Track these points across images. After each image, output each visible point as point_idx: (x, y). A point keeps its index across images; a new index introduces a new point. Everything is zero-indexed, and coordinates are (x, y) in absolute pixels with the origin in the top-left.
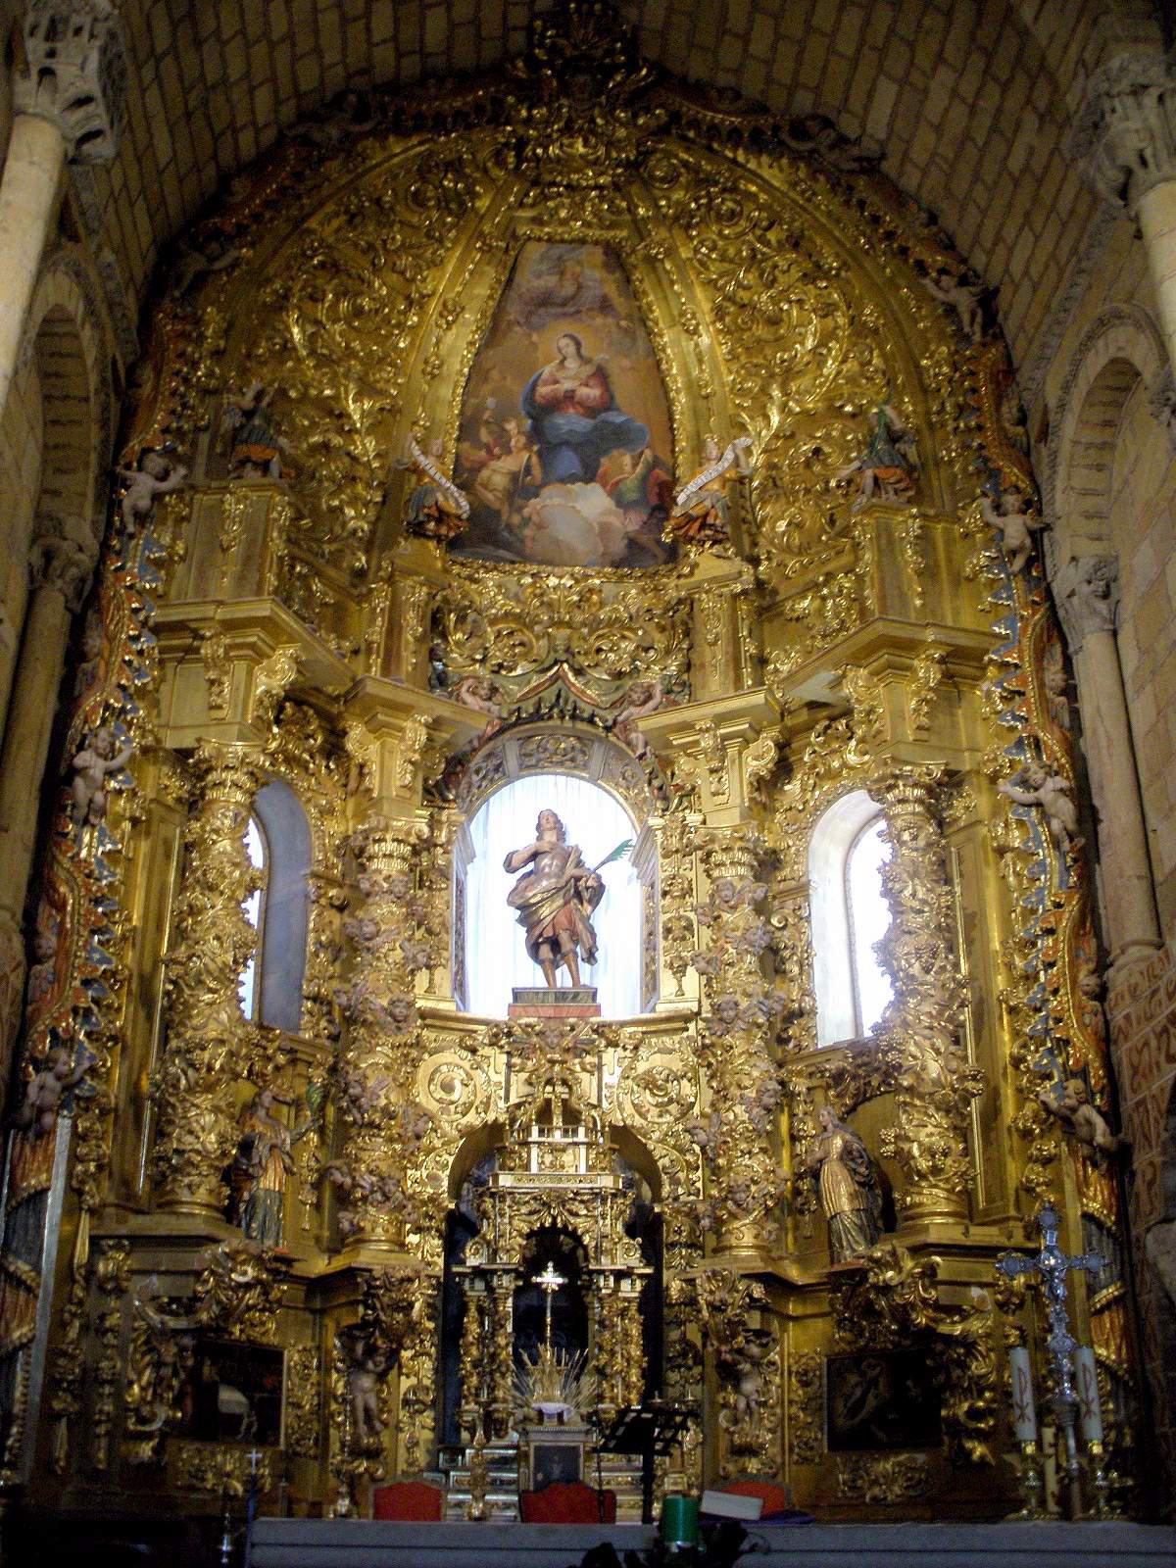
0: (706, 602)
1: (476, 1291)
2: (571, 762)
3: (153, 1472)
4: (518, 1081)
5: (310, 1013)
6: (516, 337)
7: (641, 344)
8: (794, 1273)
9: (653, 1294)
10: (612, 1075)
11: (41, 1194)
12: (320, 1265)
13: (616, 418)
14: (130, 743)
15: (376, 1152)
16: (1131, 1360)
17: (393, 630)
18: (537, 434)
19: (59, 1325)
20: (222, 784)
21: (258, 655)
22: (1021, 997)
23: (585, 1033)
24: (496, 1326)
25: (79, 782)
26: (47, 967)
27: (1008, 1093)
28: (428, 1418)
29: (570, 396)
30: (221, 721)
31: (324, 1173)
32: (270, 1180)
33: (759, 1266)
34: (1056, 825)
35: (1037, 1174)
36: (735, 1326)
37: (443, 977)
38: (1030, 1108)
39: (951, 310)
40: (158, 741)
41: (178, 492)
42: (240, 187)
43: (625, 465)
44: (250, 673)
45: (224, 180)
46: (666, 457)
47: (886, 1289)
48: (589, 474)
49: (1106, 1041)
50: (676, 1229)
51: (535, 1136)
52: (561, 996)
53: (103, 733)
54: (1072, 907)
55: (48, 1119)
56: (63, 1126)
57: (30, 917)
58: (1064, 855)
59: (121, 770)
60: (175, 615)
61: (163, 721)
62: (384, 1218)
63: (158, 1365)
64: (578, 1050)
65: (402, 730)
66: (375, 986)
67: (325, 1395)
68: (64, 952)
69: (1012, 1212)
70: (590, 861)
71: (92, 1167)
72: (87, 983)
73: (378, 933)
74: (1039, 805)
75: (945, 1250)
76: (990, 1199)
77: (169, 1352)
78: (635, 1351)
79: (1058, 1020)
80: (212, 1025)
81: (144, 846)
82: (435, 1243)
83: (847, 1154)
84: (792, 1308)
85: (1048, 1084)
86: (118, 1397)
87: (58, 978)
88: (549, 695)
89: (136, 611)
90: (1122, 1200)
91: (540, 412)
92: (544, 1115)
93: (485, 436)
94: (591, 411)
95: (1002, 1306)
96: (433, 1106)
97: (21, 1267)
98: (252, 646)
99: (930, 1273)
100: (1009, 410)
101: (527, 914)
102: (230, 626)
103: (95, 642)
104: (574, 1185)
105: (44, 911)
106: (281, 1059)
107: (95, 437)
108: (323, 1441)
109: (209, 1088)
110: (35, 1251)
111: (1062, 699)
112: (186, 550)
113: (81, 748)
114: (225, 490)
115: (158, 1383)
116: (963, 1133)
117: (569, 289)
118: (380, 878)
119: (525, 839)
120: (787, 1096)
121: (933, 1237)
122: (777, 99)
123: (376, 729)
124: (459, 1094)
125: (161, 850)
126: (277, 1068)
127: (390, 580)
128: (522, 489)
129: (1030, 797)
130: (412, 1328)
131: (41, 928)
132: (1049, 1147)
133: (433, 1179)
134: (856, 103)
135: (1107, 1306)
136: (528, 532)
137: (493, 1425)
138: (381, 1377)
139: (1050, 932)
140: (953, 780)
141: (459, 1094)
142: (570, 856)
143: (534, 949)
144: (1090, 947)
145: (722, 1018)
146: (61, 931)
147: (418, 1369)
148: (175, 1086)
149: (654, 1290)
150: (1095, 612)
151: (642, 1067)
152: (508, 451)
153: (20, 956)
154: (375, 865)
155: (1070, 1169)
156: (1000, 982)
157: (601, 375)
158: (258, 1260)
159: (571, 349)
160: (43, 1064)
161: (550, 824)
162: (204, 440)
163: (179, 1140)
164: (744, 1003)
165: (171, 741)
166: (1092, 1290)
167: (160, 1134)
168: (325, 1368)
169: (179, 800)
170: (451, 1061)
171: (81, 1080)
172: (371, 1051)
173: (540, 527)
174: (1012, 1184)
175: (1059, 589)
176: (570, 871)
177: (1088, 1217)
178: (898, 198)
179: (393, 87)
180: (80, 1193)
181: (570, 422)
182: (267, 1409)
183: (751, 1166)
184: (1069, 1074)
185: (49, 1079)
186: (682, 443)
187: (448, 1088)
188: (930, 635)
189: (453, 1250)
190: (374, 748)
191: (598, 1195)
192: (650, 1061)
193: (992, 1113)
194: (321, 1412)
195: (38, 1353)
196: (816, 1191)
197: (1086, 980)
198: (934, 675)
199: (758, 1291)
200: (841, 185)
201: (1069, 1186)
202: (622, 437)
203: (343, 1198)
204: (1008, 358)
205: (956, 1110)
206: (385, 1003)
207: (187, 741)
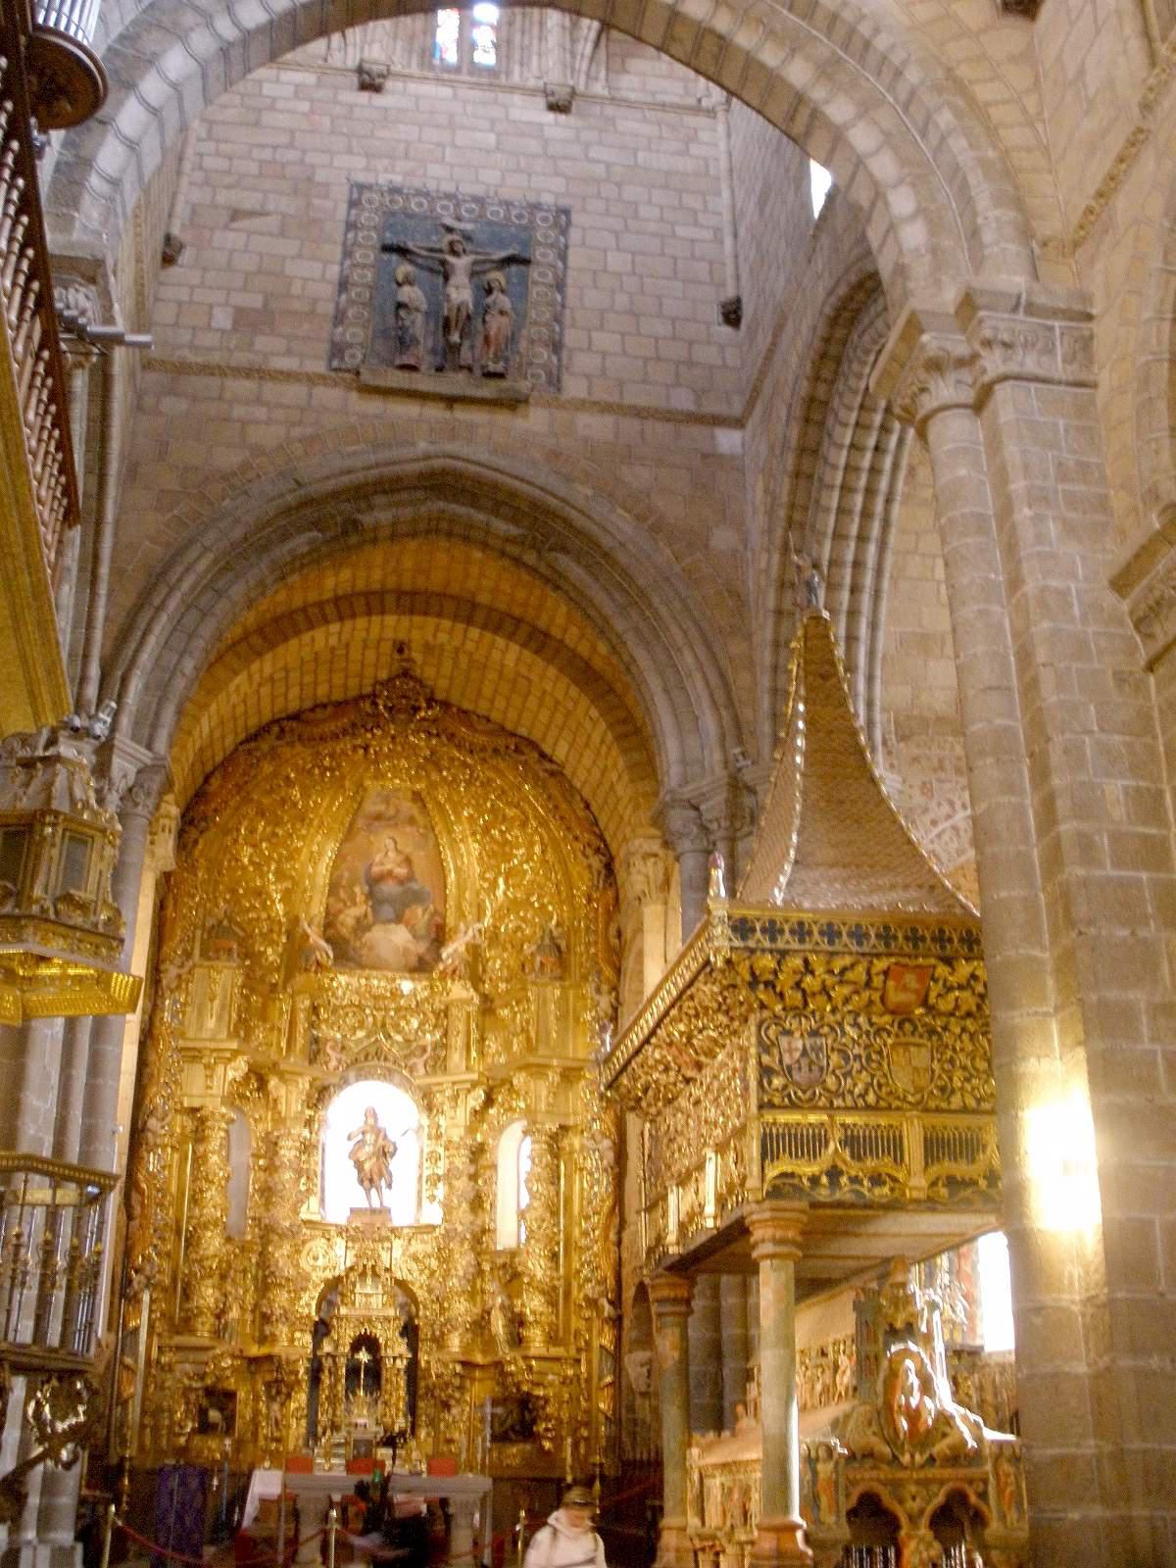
0: (454, 1011)
1: (327, 1363)
2: (388, 1075)
3: (183, 1451)
4: (351, 1254)
6: (361, 838)
7: (431, 843)
8: (479, 1359)
9: (413, 1367)
10: (397, 1253)
11: (136, 1329)
12: (255, 1351)
13: (415, 886)
15: (281, 1298)
17: (292, 1024)
18: (370, 895)
19: (146, 1386)
22: (583, 1242)
23: (384, 1232)
24: (337, 1380)
27: (575, 1284)
28: (303, 1422)
29: (390, 873)
31: (256, 1306)
32: (234, 1313)
33: (462, 1358)
35: (582, 1325)
36: (447, 1385)
37: (314, 1201)
39: (590, 866)
42: (215, 782)
43: (420, 915)
45: (207, 779)
46: (440, 908)
47: (511, 1374)
48: (398, 919)
50: (425, 1332)
51: (358, 1289)
52: (373, 1211)
54: (608, 1203)
62: (285, 1329)
63: (187, 1403)
64: (381, 1240)
66: (283, 1217)
67: (256, 1412)
68: (143, 1216)
70: (392, 1136)
75: (538, 1358)
77: (193, 1397)
78: (402, 1393)
82: (308, 1338)
83: (502, 1307)
84: (478, 1374)
86: (171, 1418)
88: (372, 1050)
90: (618, 1341)
91: (374, 882)
92: (363, 1275)
93: (342, 895)
94: (401, 882)
96: (308, 1268)
97: (128, 1361)
99: (530, 1368)
100: (612, 931)
101: (359, 1165)
103: (152, 1057)
104: (375, 1313)
108: (255, 1434)
110: (135, 1355)
115: (187, 1411)
116: (552, 1303)
117: (392, 812)
119: (357, 1123)
120: (480, 1272)
121: (533, 1352)
122: (509, 726)
124: (321, 1262)
127: (292, 996)
128: (361, 926)
130: (298, 1382)
132: (587, 1314)
133: (308, 1305)
134: (550, 740)
136: (364, 952)
137: (335, 1427)
138: (283, 1405)
140: (564, 1128)
141: (321, 1262)
142: (378, 1132)
143: (361, 1182)
144: (616, 1221)
145: (448, 1235)
146: (142, 1204)
147: (301, 1398)
149: (413, 1364)
151: (412, 1249)
152: (354, 904)
155: (596, 1324)
156: (576, 1232)
157: (408, 861)
158: (234, 1357)
159: (391, 845)
161: (372, 1114)
163: (196, 1302)
164: (460, 1228)
166: (600, 1378)
168: (257, 1398)
170: (318, 1245)
173: (371, 948)
176: (381, 1142)
178: (569, 790)
179: (296, 717)
181: (389, 888)
182: (230, 1420)
183: (461, 1308)
184: (599, 1283)
186: (451, 902)
187: (316, 1259)
188: (555, 1062)
189: (317, 1345)
190: (283, 1091)
191: (387, 1319)
192: (417, 1247)
193: (567, 1294)
194: (255, 1423)
195: (138, 1400)
196: (489, 1322)
197: (612, 1236)
198: (557, 1079)
199: (458, 1368)
200: (537, 782)
202: (418, 897)
203: (266, 1318)
204: (617, 898)
205: (550, 1295)
207: (196, 1104)
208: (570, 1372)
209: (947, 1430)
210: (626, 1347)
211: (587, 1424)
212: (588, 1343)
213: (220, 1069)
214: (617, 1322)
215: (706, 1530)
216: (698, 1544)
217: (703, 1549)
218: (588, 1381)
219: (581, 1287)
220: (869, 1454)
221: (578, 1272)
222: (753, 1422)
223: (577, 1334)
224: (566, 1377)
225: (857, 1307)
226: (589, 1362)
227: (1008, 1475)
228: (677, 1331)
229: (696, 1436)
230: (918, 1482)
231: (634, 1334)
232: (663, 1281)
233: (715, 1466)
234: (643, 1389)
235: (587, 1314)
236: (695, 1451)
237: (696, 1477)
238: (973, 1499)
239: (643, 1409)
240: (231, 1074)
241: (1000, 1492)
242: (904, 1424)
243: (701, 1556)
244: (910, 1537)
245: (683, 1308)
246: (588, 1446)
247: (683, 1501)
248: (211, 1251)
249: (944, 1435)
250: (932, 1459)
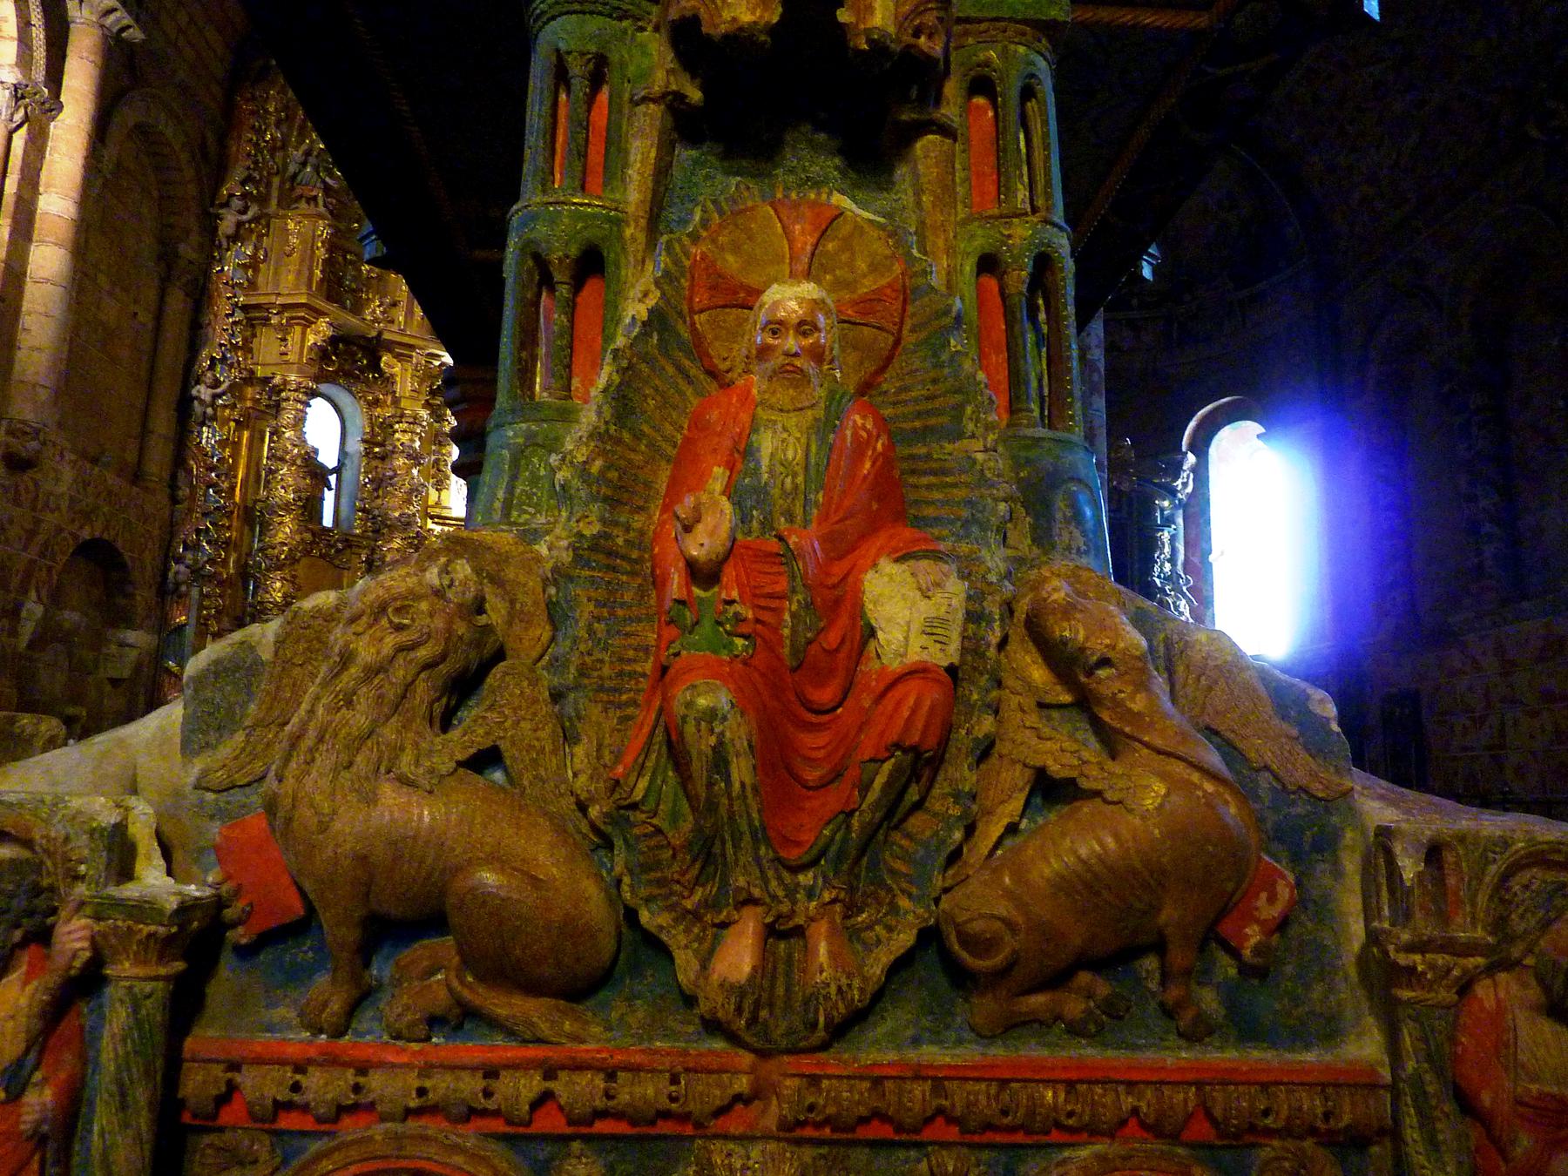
5: (361, 519)
14: (226, 377)
20: (287, 399)
21: (308, 324)
25: (196, 402)
26: (186, 504)
30: (286, 363)
40: (252, 372)
41: (256, 219)
44: (304, 334)
53: (209, 374)
55: (184, 588)
56: (195, 593)
57: (174, 477)
59: (224, 393)
60: (254, 301)
61: (255, 360)
65: (411, 357)
68: (193, 497)
71: (213, 611)
72: (205, 515)
73: (396, 475)
80: (281, 535)
81: (246, 434)
87: (190, 510)
89: (229, 298)
98: (303, 318)
102: (285, 307)
105: (181, 475)
106: (340, 546)
107: (192, 190)
109: (279, 568)
112: (266, 255)
113: (198, 382)
114: (285, 217)
118: (398, 444)
123: (398, 357)
125: (257, 435)
126: (338, 551)
131: (180, 484)
148: (260, 568)
153: (166, 501)
154: (397, 435)
160: (179, 560)
162: (276, 181)
165: (260, 372)
167: (255, 593)
169: (267, 406)
171: (204, 567)
172: (390, 541)
180: (206, 625)
185: (182, 568)
206: (397, 514)
213: (298, 329)
240: (311, 339)
248: (280, 537)
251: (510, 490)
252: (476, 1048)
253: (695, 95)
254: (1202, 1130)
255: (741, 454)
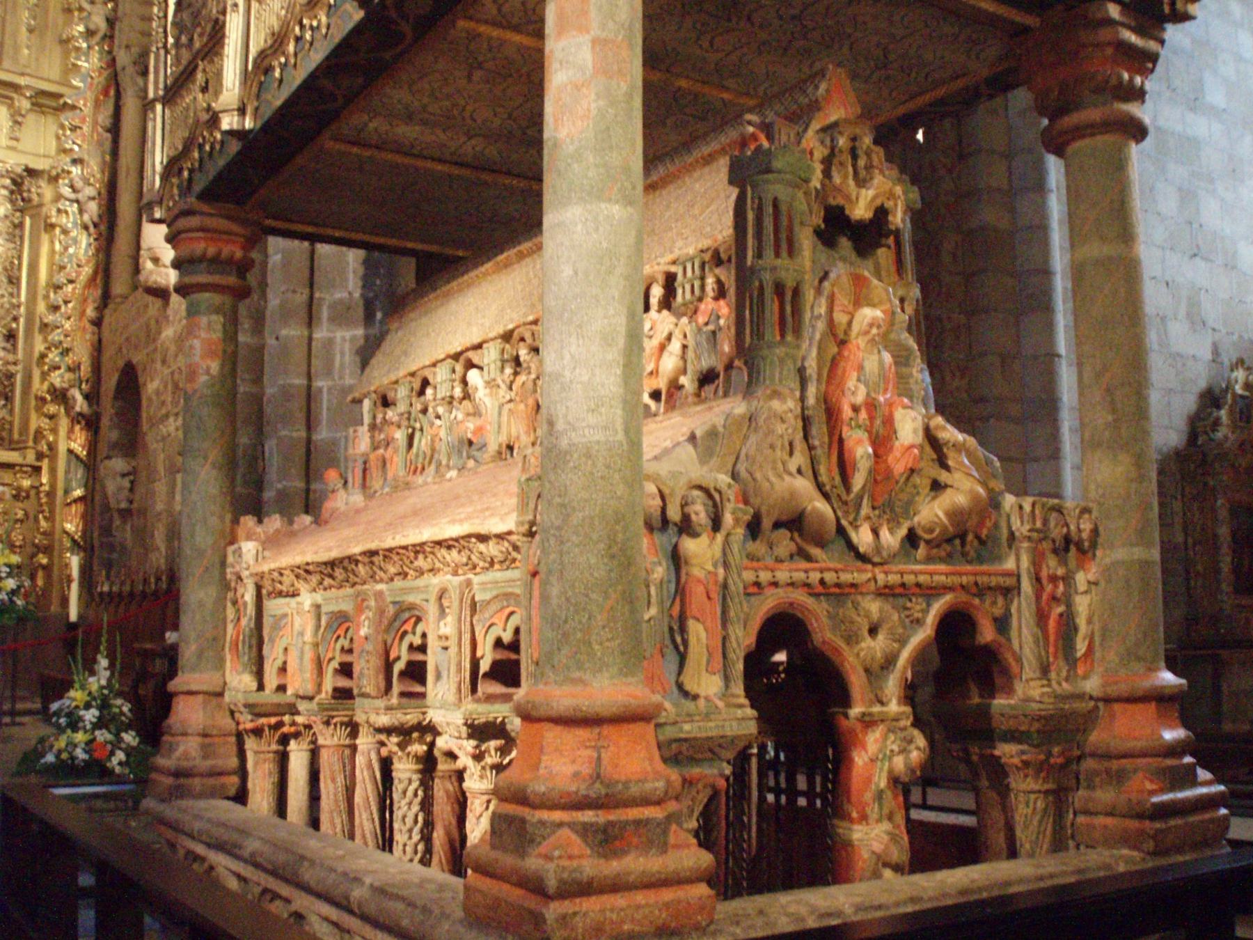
16: (84, 532)
22: (50, 318)
27: (36, 374)
34: (86, 217)
35: (45, 423)
38: (45, 386)
49: (98, 348)
54: (87, 271)
58: (89, 235)
69: (31, 444)
74: (77, 201)
76: (21, 434)
79: (66, 336)
85: (57, 372)
90: (92, 447)
95: (16, 497)
111: (109, 135)
129: (73, 196)
135: (75, 501)
139: (71, 282)
150: (135, 84)
155: (64, 423)
156: (41, 307)
166: (67, 492)
174: (33, 426)
175: (119, 64)
177: (70, 451)
184: (70, 369)
197: (90, 312)
201: (63, 431)
208: (26, 483)
209: (944, 476)
210: (103, 449)
211: (48, 550)
212: (52, 447)
214: (91, 423)
215: (269, 696)
216: (247, 722)
217: (257, 732)
218: (51, 494)
219: (44, 376)
220: (795, 522)
221: (43, 356)
222: (357, 498)
223: (39, 434)
224: (19, 489)
225: (738, 176)
226: (53, 471)
227: (1053, 579)
228: (218, 320)
229: (248, 521)
230: (886, 593)
231: (114, 435)
232: (194, 221)
233: (304, 571)
234: (123, 505)
235: (52, 408)
236: (249, 548)
237: (249, 596)
238: (987, 634)
239: (124, 533)
241: (1041, 617)
242: (861, 450)
243: (250, 744)
244: (868, 722)
245: (232, 280)
246: (48, 577)
247: (217, 641)
249: (937, 486)
250: (912, 539)
251: (781, 373)
252: (804, 565)
253: (823, 226)
254: (974, 590)
255: (861, 368)
